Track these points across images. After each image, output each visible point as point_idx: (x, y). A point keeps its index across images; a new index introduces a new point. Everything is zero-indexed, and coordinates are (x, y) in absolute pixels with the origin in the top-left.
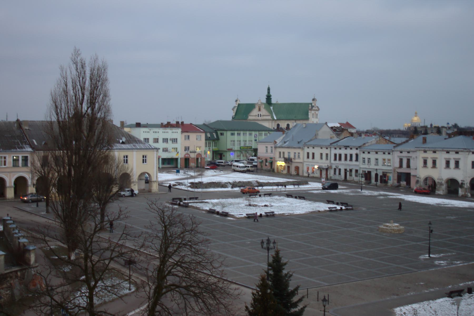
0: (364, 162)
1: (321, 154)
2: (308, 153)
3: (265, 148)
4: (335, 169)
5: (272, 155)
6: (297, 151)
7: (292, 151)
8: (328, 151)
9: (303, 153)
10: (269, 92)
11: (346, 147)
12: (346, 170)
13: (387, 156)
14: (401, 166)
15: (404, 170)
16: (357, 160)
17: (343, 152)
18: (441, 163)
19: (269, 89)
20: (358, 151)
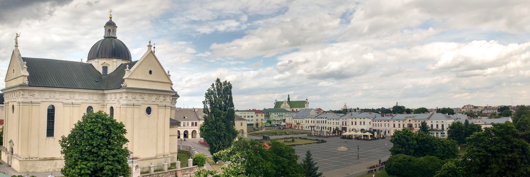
0: (328, 123)
1: (312, 121)
2: (306, 121)
3: (289, 119)
4: (317, 127)
5: (291, 122)
6: (302, 120)
7: (300, 120)
8: (314, 120)
9: (304, 121)
10: (289, 97)
11: (321, 118)
12: (321, 127)
13: (337, 121)
14: (343, 125)
15: (344, 126)
16: (326, 123)
17: (320, 120)
18: (358, 123)
19: (289, 95)
20: (326, 119)
